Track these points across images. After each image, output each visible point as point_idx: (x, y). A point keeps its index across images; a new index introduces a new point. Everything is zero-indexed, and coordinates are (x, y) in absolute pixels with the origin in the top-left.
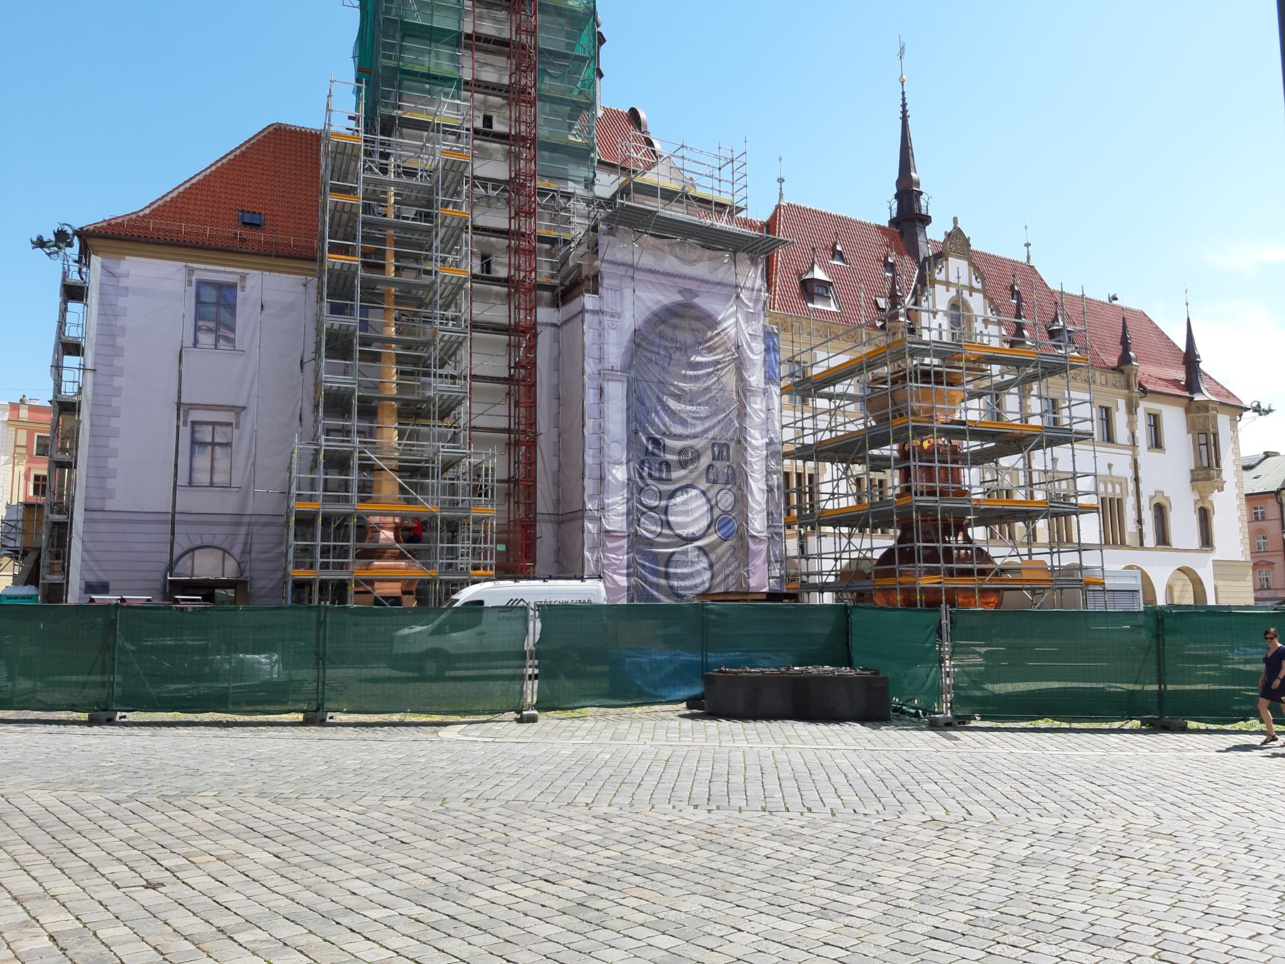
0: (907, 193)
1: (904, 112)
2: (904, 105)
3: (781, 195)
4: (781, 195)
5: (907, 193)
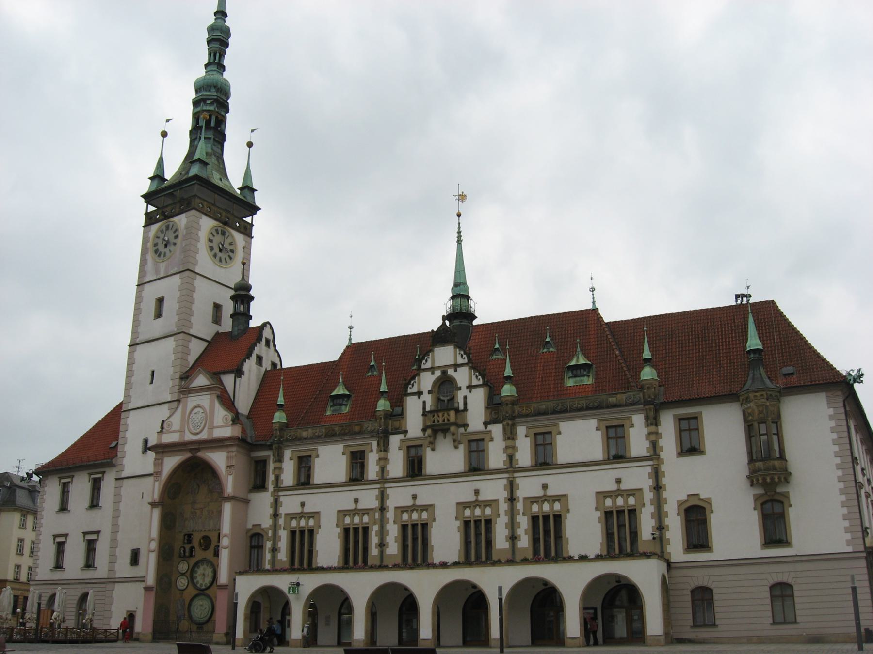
0: (460, 294)
1: (459, 237)
2: (459, 232)
3: (350, 339)
4: (350, 339)
5: (460, 294)
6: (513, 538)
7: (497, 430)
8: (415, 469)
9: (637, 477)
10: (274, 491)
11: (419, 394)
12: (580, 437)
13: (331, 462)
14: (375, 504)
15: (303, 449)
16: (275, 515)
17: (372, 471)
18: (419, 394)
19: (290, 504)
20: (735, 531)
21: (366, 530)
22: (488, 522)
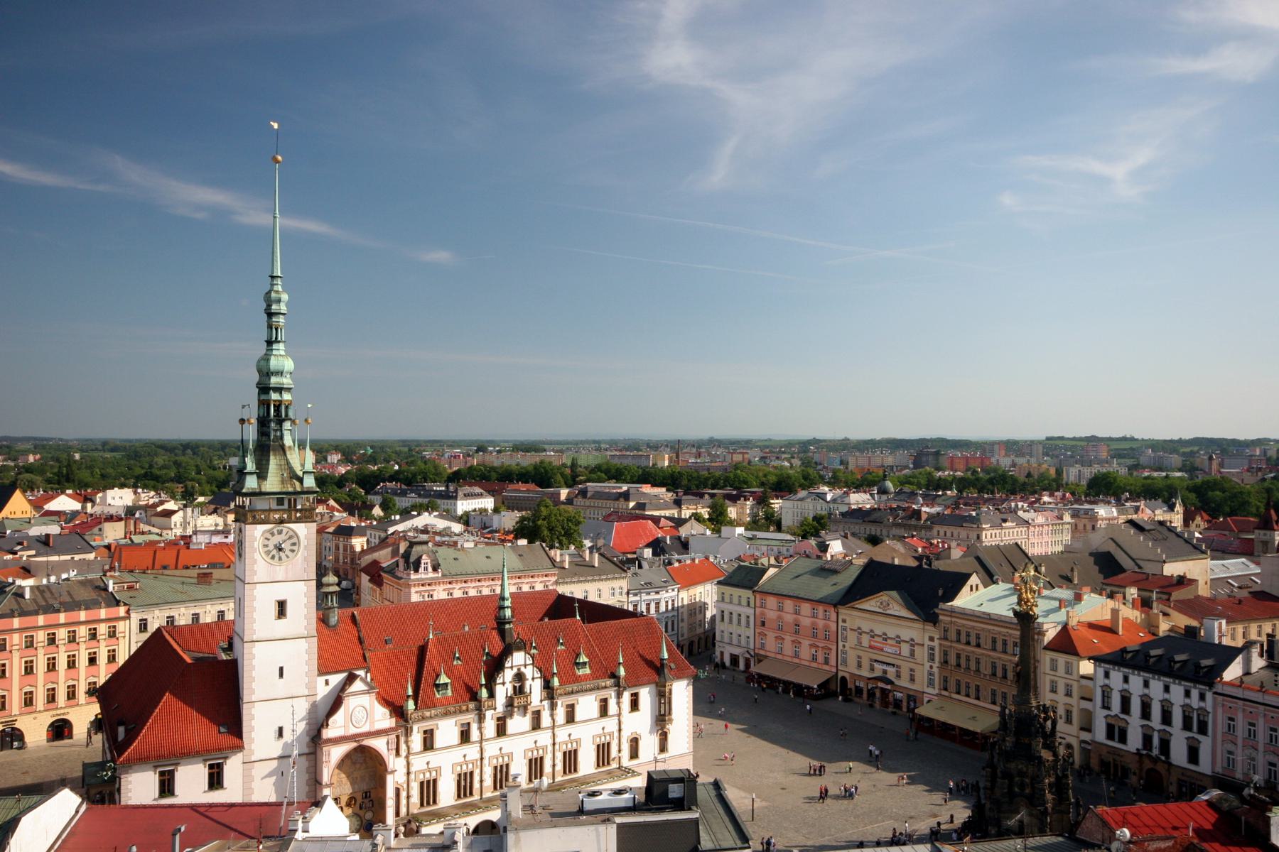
6: (554, 766)
7: (546, 703)
8: (501, 731)
9: (610, 724)
10: (407, 757)
11: (503, 684)
12: (587, 705)
13: (447, 730)
14: (478, 756)
15: (427, 725)
16: (408, 773)
17: (475, 735)
18: (503, 684)
19: (419, 763)
20: (649, 745)
21: (472, 773)
22: (542, 758)
